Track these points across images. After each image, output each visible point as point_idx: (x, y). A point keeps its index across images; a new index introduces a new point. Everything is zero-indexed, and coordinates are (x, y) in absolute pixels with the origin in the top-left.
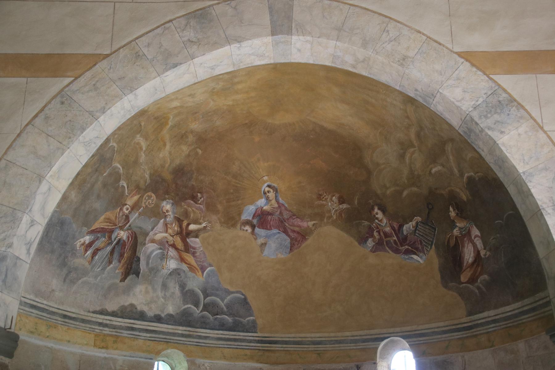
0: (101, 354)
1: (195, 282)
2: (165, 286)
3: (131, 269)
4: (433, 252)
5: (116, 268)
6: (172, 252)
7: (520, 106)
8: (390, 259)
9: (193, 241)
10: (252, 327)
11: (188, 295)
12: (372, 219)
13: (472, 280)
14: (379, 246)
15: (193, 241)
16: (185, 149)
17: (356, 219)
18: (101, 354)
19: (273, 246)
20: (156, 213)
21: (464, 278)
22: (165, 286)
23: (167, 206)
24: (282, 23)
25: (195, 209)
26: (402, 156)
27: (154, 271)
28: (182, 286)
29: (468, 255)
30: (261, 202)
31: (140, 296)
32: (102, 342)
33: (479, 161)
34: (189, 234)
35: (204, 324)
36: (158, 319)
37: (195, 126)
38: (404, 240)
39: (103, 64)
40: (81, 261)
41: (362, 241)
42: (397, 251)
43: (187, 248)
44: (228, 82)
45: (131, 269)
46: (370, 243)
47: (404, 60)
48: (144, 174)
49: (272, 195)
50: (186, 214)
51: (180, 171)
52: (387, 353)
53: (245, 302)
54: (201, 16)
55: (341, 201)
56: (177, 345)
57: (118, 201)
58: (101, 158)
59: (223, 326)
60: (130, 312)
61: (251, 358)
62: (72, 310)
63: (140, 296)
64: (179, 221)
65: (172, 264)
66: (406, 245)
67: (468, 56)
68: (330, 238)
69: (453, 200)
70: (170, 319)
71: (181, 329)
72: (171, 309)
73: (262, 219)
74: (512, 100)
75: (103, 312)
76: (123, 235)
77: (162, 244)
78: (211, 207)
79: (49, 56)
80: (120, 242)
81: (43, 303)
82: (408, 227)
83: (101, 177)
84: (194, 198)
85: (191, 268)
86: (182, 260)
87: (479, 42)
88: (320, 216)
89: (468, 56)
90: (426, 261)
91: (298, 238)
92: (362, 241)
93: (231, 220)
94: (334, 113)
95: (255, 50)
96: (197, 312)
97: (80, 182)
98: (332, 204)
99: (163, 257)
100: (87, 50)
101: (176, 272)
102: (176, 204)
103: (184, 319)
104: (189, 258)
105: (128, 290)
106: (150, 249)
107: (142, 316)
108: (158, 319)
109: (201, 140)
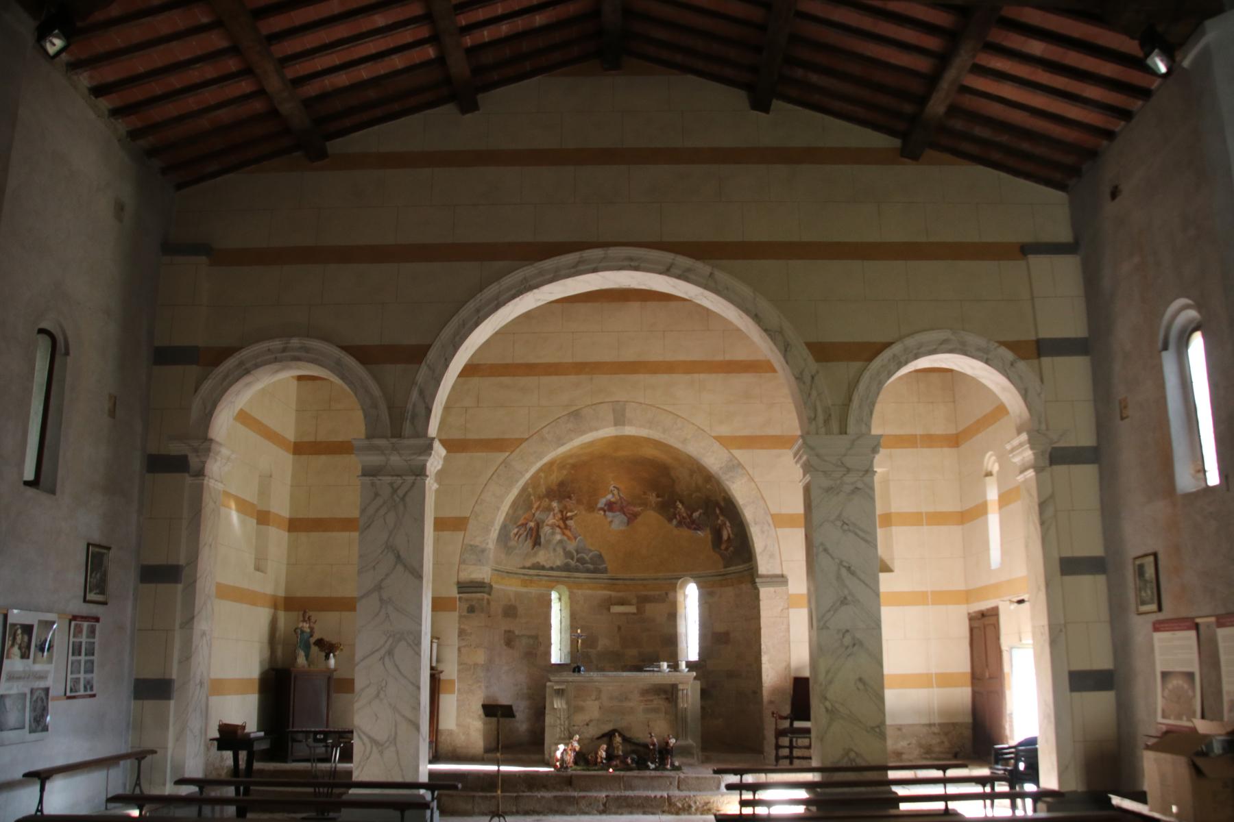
0: (524, 590)
1: (572, 546)
2: (555, 550)
3: (537, 543)
4: (708, 531)
5: (529, 543)
6: (558, 530)
7: (743, 468)
8: (686, 532)
9: (569, 522)
10: (605, 571)
11: (568, 554)
12: (676, 508)
13: (727, 549)
14: (680, 524)
15: (569, 522)
16: (565, 472)
17: (667, 507)
18: (524, 590)
19: (617, 522)
20: (549, 509)
21: (723, 547)
22: (555, 550)
23: (555, 504)
24: (619, 421)
25: (570, 503)
26: (691, 476)
27: (549, 542)
28: (564, 549)
29: (725, 537)
30: (610, 497)
31: (542, 557)
32: (525, 584)
33: (724, 491)
34: (567, 518)
35: (577, 570)
36: (552, 569)
37: (571, 461)
38: (693, 522)
39: (524, 445)
40: (513, 543)
41: (670, 520)
42: (689, 528)
43: (566, 527)
44: (592, 443)
45: (537, 543)
46: (675, 522)
47: (684, 441)
48: (543, 490)
49: (616, 492)
50: (565, 507)
51: (562, 484)
52: (684, 586)
53: (600, 556)
54: (576, 415)
55: (658, 496)
56: (563, 583)
57: (530, 507)
58: (524, 489)
59: (588, 571)
60: (538, 566)
61: (604, 589)
62: (509, 568)
63: (542, 557)
64: (561, 511)
65: (558, 537)
66: (694, 525)
67: (719, 439)
68: (651, 518)
69: (717, 504)
70: (559, 569)
71: (564, 574)
72: (558, 563)
73: (610, 506)
74: (740, 464)
75: (524, 568)
76: (532, 524)
77: (553, 526)
78: (579, 502)
79: (497, 440)
80: (531, 529)
81: (499, 567)
82: (696, 515)
83: (524, 501)
84: (570, 498)
85: (569, 538)
86: (564, 534)
87: (725, 430)
88: (645, 504)
89: (719, 439)
90: (704, 535)
91: (632, 518)
92: (670, 520)
93: (591, 508)
94: (649, 452)
95: (608, 432)
96: (573, 563)
97: (514, 505)
98: (652, 498)
99: (553, 534)
100: (517, 436)
101: (561, 541)
102: (559, 502)
103: (566, 568)
104: (567, 532)
105: (535, 554)
106: (546, 530)
107: (543, 568)
108: (552, 569)
109: (574, 466)
